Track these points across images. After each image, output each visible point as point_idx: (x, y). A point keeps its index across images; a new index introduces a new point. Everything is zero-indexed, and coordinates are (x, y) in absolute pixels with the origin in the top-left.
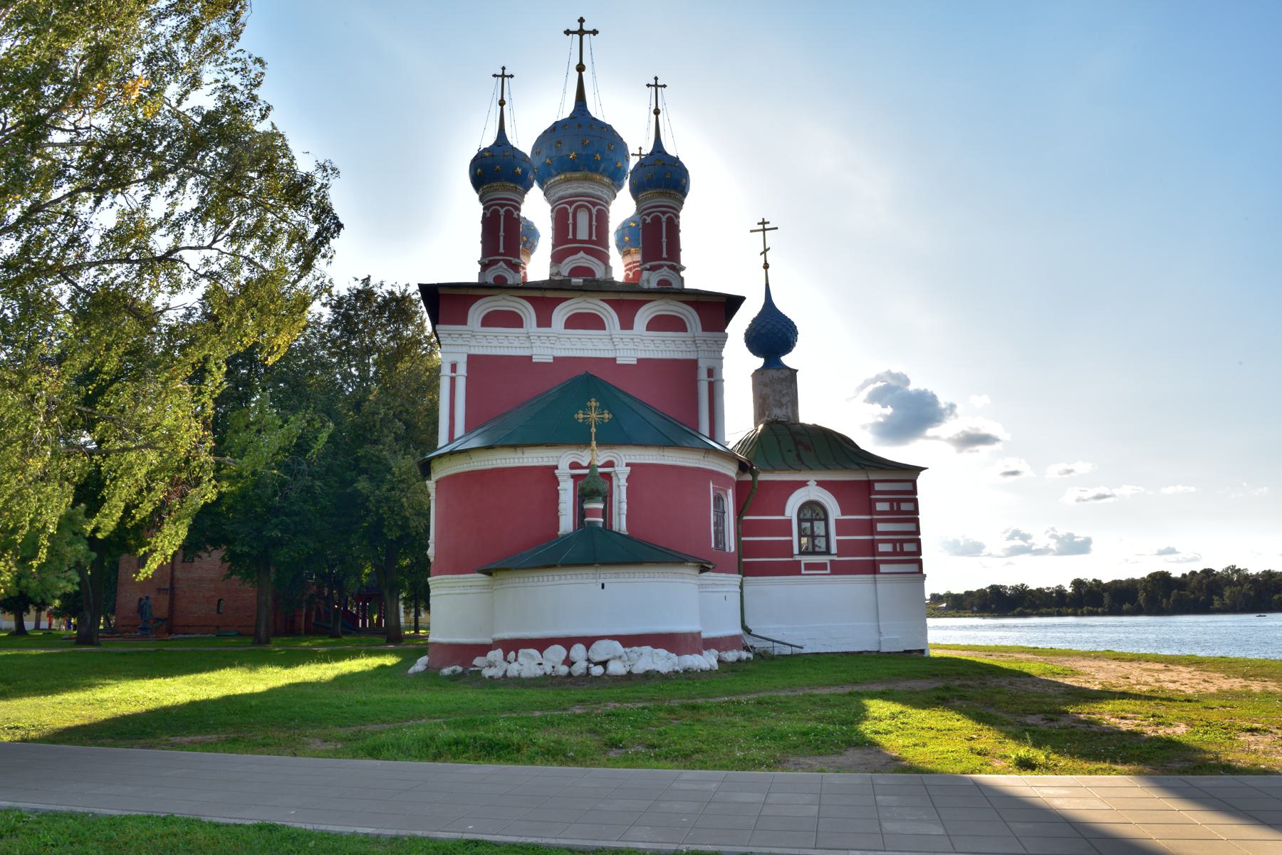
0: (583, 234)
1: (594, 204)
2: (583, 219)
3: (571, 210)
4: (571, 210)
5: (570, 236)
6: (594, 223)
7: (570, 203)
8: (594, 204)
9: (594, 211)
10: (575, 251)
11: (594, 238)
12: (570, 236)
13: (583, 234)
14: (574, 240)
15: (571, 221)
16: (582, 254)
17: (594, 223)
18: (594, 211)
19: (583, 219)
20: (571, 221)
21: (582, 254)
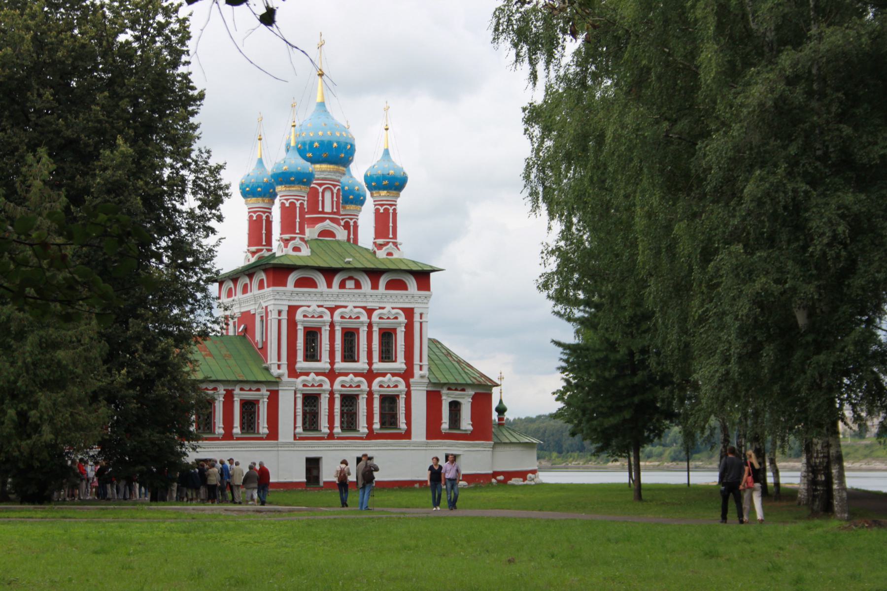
0: (328, 209)
1: (335, 186)
2: (328, 195)
3: (321, 190)
4: (321, 190)
5: (320, 209)
6: (335, 199)
7: (320, 185)
8: (335, 186)
9: (335, 191)
10: (323, 220)
11: (335, 210)
12: (320, 209)
13: (328, 209)
14: (323, 212)
15: (320, 198)
16: (328, 221)
17: (335, 199)
18: (335, 191)
19: (328, 195)
20: (320, 198)
21: (328, 221)
